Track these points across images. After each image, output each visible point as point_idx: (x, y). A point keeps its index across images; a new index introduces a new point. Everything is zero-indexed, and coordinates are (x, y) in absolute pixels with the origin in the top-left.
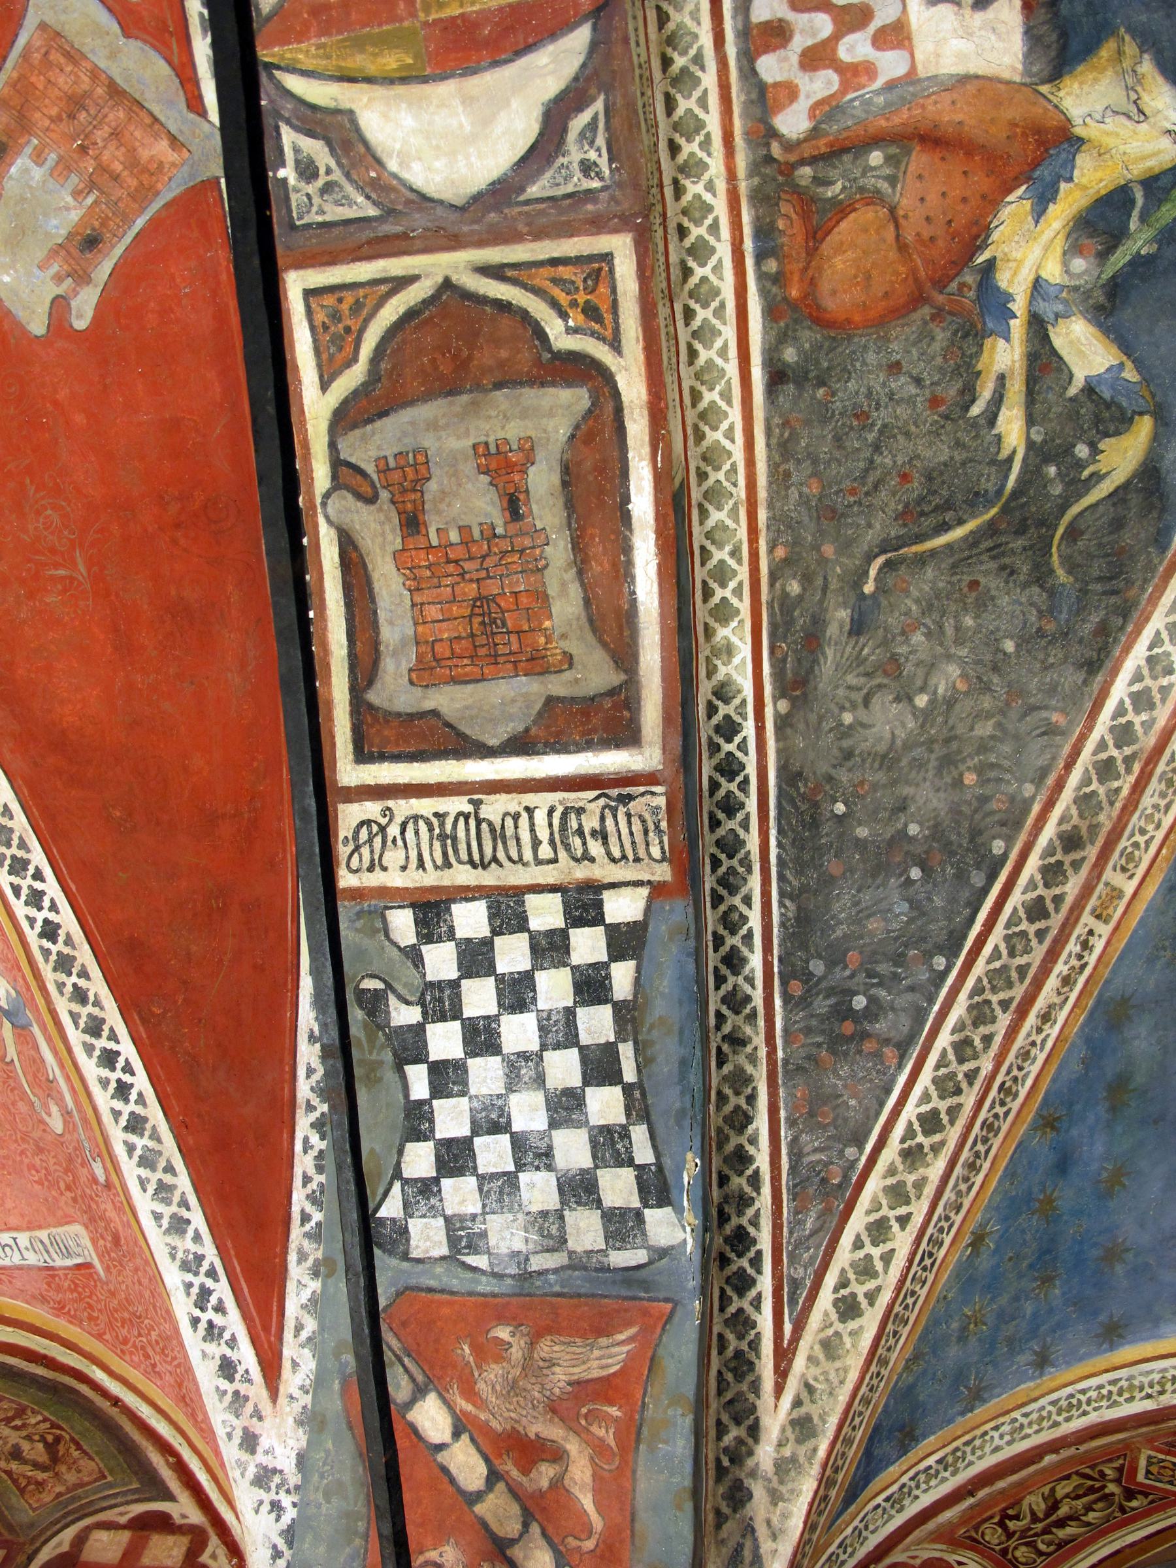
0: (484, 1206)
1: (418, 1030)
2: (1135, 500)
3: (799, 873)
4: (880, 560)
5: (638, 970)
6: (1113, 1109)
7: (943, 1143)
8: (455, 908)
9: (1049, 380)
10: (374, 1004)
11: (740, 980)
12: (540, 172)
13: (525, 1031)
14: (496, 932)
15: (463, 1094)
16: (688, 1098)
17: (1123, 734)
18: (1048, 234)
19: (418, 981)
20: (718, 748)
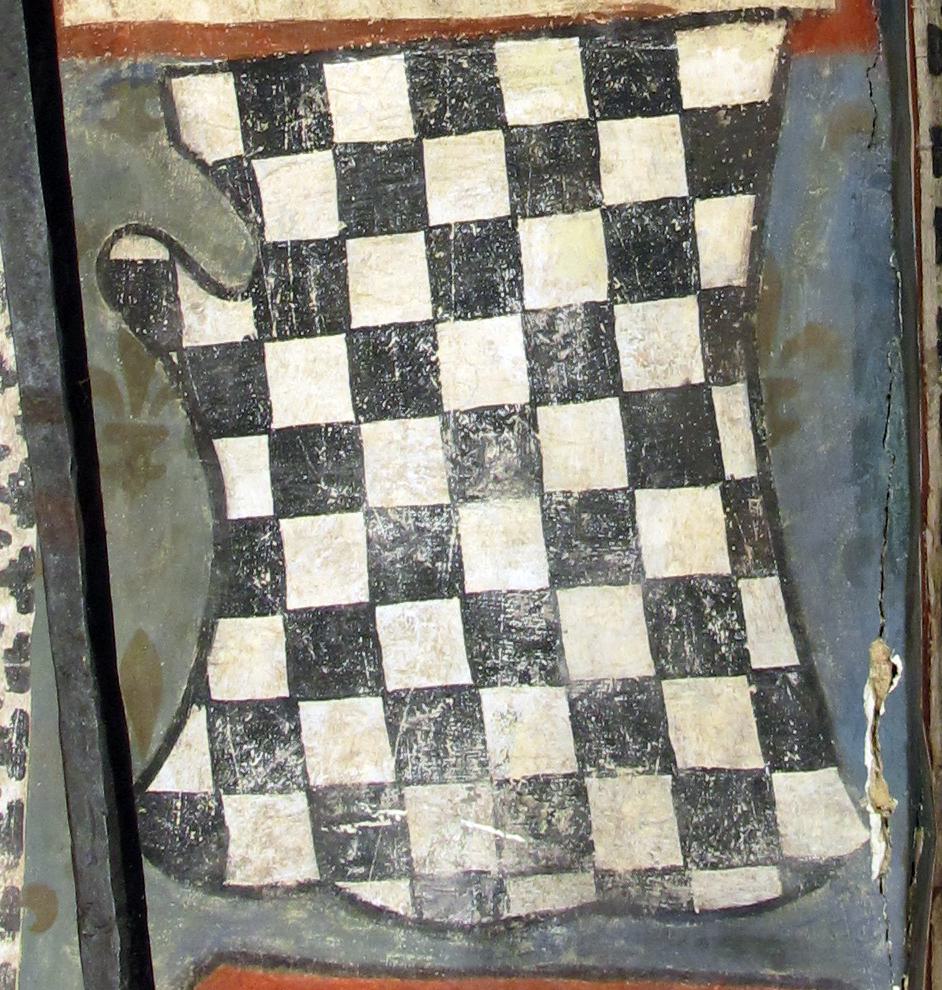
0: (400, 766)
1: (248, 357)
5: (759, 216)
10: (145, 295)
13: (496, 359)
14: (428, 128)
15: (352, 504)
16: (874, 514)
19: (245, 242)
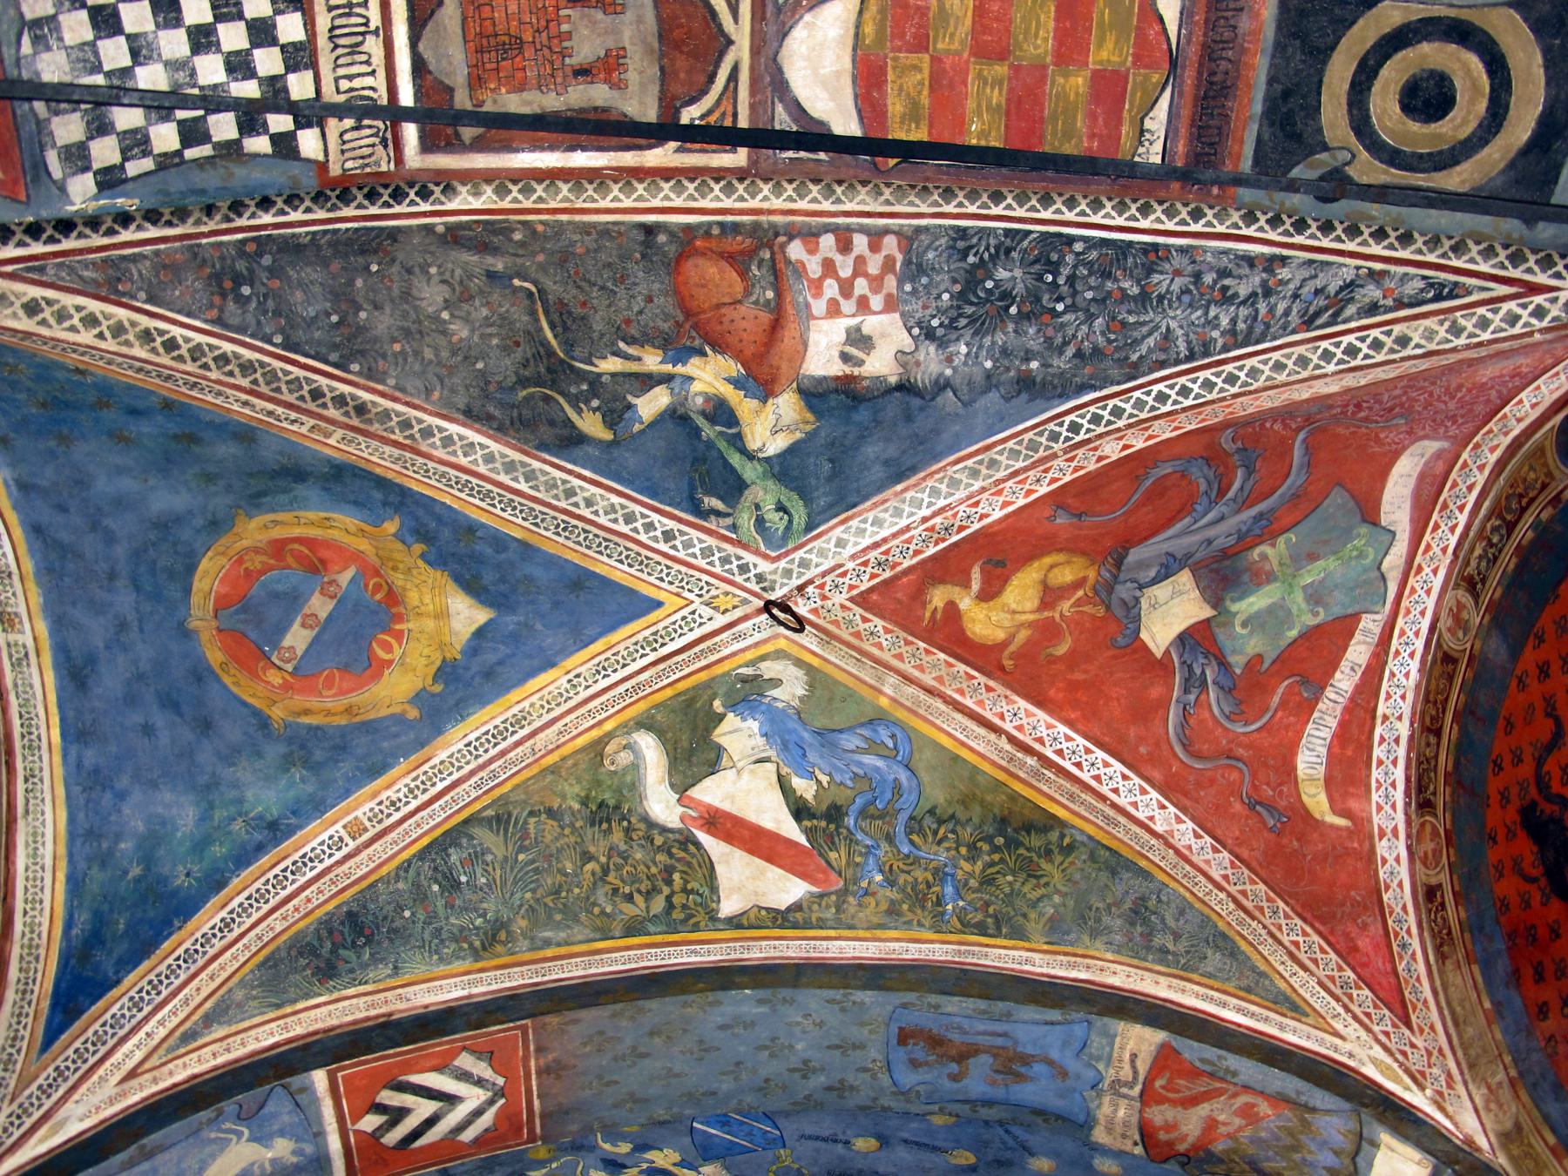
2: (566, 432)
3: (330, 244)
4: (534, 289)
5: (266, 155)
6: (176, 437)
7: (158, 354)
8: (298, 15)
9: (637, 385)
11: (253, 209)
12: (790, 114)
14: (283, 47)
15: (157, 25)
17: (427, 433)
18: (717, 385)
20: (411, 187)
